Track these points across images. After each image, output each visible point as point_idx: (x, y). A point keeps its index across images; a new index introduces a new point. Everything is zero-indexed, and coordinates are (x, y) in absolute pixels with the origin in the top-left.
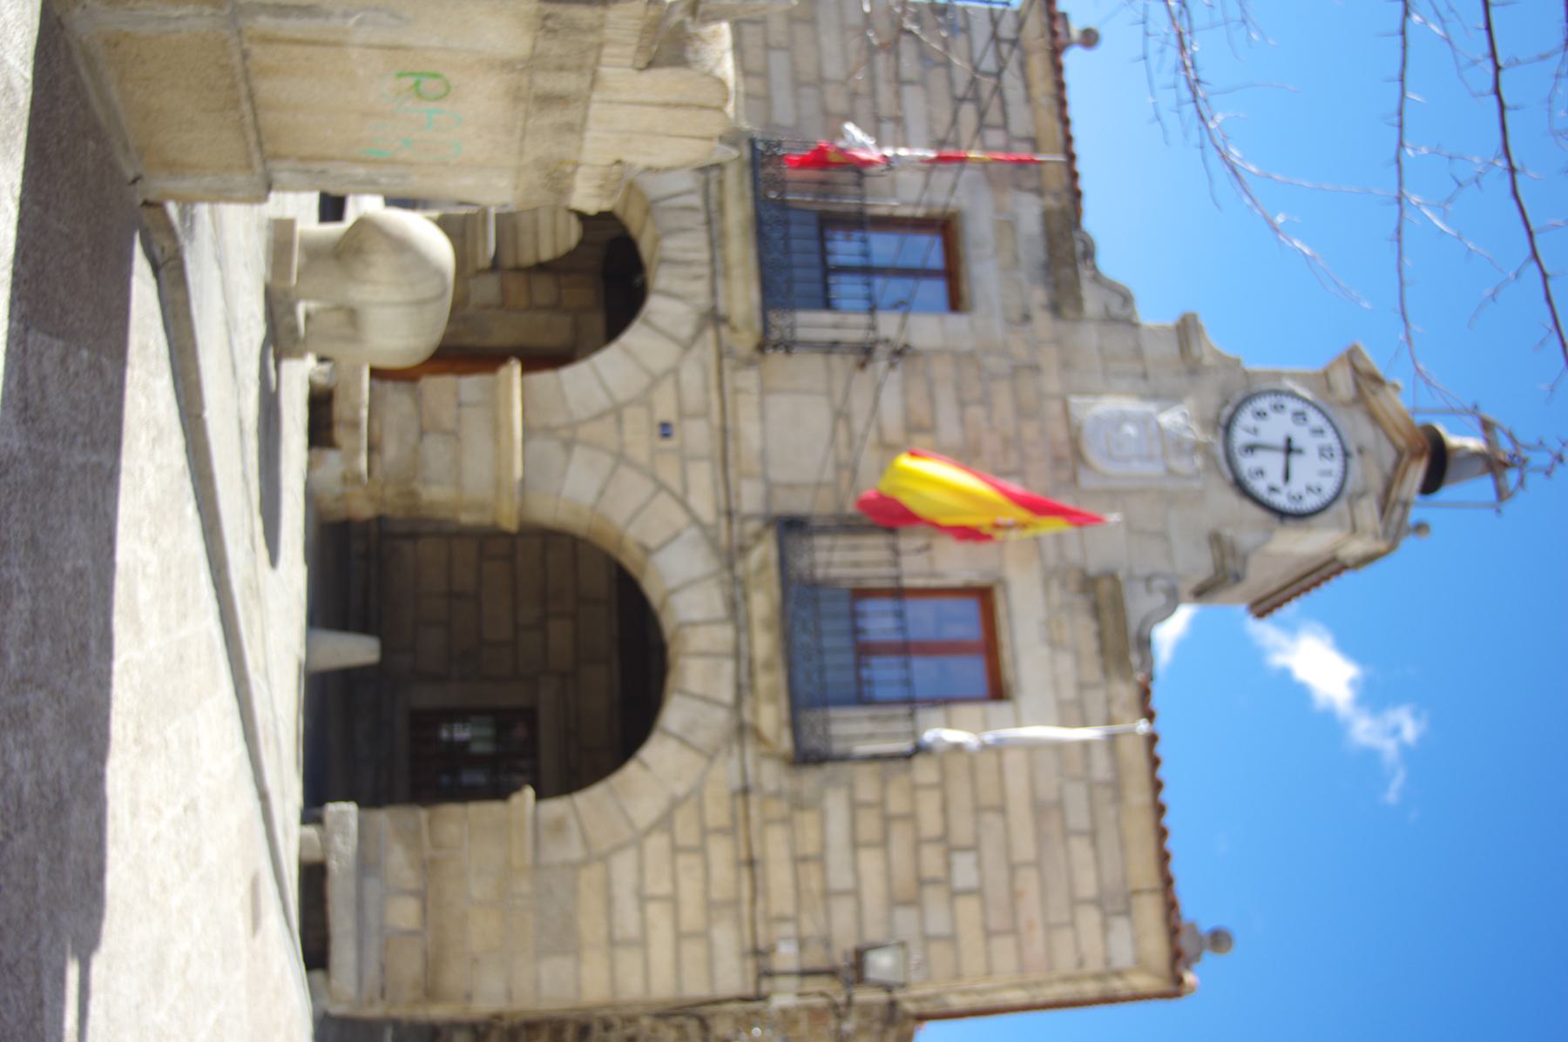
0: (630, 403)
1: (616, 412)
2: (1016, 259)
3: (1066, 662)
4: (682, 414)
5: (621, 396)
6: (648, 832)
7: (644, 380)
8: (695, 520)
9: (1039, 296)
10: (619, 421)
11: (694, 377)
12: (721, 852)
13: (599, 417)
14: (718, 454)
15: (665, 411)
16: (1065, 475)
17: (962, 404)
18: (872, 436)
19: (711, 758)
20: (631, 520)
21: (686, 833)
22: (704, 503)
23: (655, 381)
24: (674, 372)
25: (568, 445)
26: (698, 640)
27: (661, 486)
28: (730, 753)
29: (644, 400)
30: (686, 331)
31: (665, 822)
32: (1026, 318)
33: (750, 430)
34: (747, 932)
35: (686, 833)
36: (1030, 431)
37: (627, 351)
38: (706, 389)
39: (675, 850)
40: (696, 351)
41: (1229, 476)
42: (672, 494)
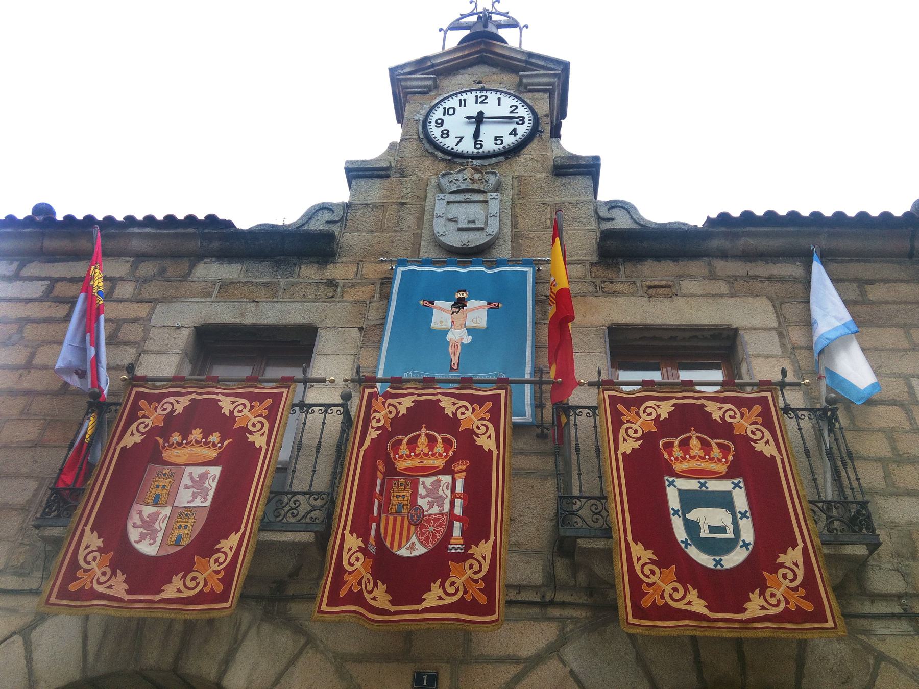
3: (688, 286)
8: (554, 650)
9: (309, 272)
19: (881, 658)
28: (869, 633)
30: (285, 641)
32: (331, 283)
41: (502, 158)
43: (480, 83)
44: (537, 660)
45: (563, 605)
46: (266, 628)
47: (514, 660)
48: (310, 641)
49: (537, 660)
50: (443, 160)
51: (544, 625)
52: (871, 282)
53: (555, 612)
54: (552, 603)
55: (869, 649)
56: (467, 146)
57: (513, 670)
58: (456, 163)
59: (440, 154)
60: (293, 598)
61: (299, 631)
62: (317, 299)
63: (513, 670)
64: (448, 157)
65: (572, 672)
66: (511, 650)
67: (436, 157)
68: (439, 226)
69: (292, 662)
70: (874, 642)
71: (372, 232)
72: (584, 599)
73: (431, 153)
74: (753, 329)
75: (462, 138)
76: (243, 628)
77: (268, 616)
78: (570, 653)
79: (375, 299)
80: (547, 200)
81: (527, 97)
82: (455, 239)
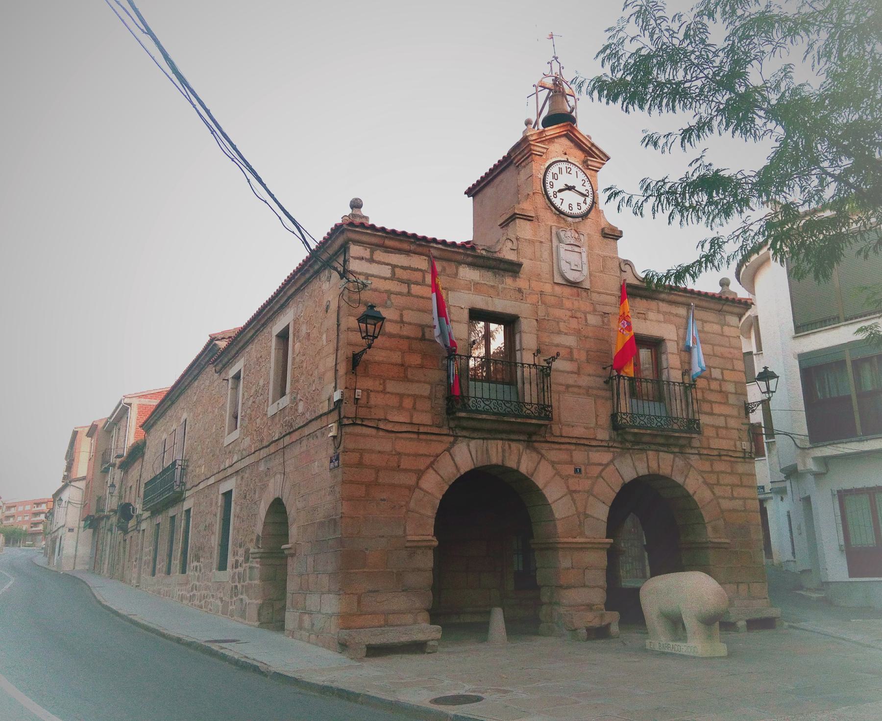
0: (568, 487)
1: (571, 492)
2: (492, 286)
4: (571, 463)
7: (557, 478)
8: (612, 461)
9: (509, 281)
10: (575, 491)
11: (554, 455)
12: (720, 466)
13: (574, 500)
14: (586, 448)
15: (569, 470)
16: (584, 294)
17: (559, 332)
19: (691, 466)
20: (614, 491)
21: (712, 479)
22: (606, 457)
23: (558, 473)
24: (553, 463)
25: (587, 516)
26: (654, 465)
27: (600, 475)
28: (689, 459)
29: (566, 478)
30: (534, 455)
31: (710, 486)
32: (520, 290)
33: (579, 431)
34: (739, 460)
35: (712, 479)
36: (567, 304)
37: (545, 486)
38: (560, 449)
39: (718, 484)
40: (543, 452)
41: (581, 219)
42: (603, 470)
43: (565, 154)
44: (607, 465)
45: (615, 447)
46: (528, 451)
47: (600, 464)
48: (542, 456)
49: (607, 465)
50: (555, 214)
51: (609, 454)
52: (706, 322)
53: (612, 449)
54: (612, 447)
55: (689, 463)
56: (551, 192)
57: (601, 468)
58: (560, 217)
59: (553, 209)
60: (536, 441)
61: (538, 452)
62: (516, 300)
63: (601, 468)
64: (558, 213)
65: (617, 469)
66: (600, 461)
67: (552, 210)
68: (565, 267)
69: (539, 463)
71: (531, 259)
73: (549, 207)
74: (670, 340)
75: (563, 200)
76: (521, 451)
77: (528, 447)
78: (616, 462)
79: (540, 303)
80: (601, 253)
81: (588, 172)
82: (572, 276)
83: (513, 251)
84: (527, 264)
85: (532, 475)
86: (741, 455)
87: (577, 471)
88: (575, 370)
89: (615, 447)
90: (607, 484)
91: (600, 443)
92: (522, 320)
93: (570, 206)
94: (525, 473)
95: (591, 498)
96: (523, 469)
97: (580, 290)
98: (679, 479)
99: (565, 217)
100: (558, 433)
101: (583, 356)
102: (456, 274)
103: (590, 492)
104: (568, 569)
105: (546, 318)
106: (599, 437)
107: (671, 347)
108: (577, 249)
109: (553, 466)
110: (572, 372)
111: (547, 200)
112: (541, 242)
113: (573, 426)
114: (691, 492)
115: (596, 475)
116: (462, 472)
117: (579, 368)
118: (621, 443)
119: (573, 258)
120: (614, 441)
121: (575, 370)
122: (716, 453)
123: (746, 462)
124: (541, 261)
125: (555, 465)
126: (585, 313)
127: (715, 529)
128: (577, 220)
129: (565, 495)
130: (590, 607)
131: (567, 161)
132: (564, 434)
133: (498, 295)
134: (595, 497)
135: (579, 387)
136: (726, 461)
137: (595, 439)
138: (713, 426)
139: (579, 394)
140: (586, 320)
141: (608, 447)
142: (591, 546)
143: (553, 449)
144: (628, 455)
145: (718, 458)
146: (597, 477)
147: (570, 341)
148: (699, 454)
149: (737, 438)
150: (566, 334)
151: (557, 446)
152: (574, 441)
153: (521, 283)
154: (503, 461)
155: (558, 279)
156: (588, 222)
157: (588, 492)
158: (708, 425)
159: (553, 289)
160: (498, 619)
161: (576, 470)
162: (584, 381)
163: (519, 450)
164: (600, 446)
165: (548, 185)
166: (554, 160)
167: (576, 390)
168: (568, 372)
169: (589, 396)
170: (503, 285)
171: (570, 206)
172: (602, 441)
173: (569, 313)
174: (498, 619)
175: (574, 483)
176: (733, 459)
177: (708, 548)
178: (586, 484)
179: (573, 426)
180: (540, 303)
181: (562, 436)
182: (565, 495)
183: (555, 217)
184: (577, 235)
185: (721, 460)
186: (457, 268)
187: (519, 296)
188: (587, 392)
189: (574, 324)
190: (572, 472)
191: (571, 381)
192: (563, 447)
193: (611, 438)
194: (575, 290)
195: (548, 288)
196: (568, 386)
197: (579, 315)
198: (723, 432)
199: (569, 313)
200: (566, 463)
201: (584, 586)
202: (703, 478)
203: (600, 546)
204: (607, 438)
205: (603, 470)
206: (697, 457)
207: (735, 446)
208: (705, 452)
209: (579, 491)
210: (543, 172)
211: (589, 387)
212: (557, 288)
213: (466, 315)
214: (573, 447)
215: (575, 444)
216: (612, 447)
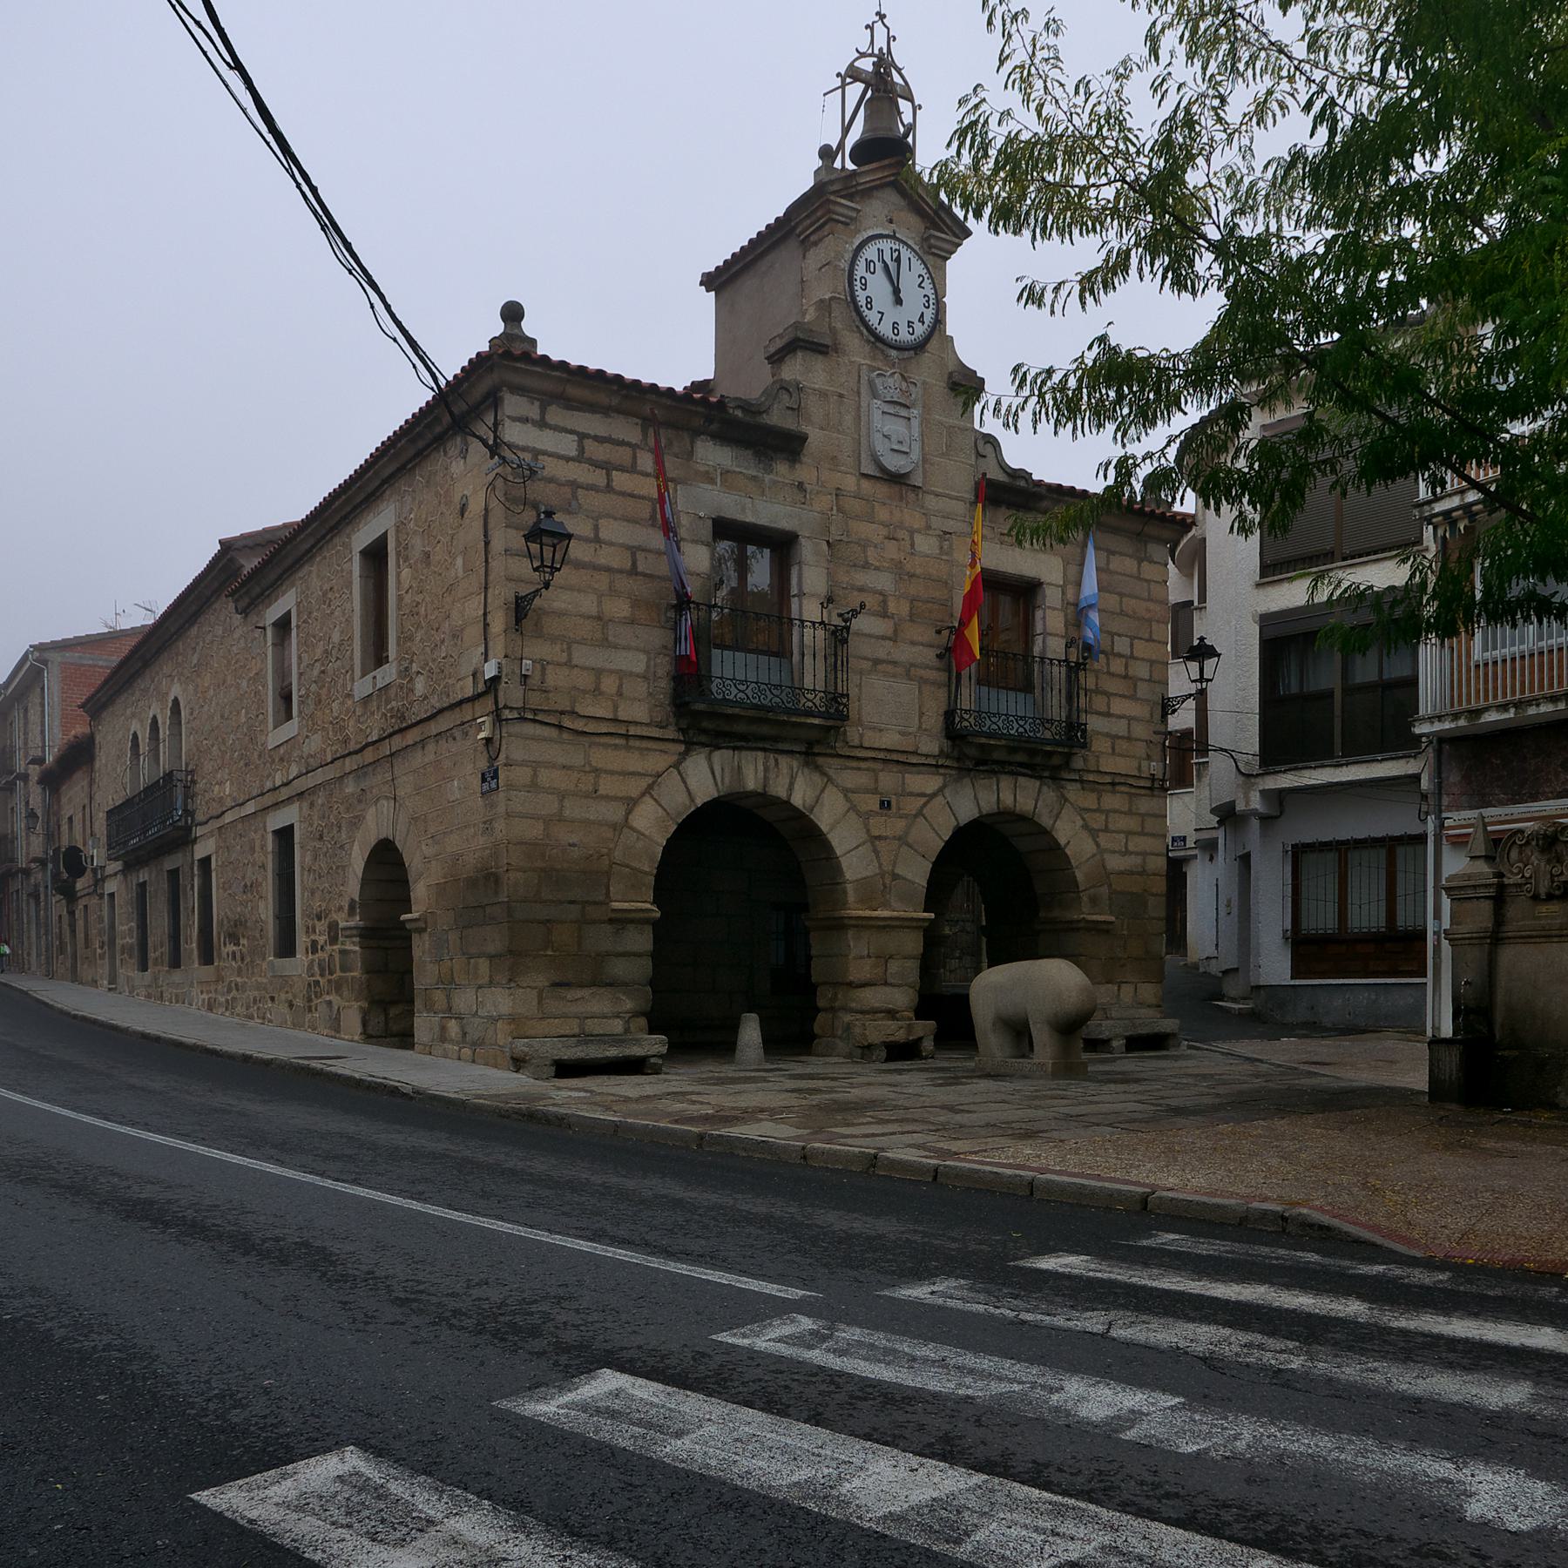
0: (868, 831)
2: (754, 478)
4: (875, 791)
5: (863, 836)
6: (1098, 845)
7: (852, 815)
8: (941, 790)
9: (781, 468)
10: (879, 838)
11: (851, 778)
12: (1112, 801)
13: (876, 852)
14: (900, 767)
15: (873, 803)
16: (911, 496)
17: (866, 566)
18: (888, 643)
19: (1066, 800)
21: (1097, 821)
22: (931, 783)
23: (853, 808)
24: (846, 792)
25: (895, 877)
26: (1007, 799)
27: (920, 813)
29: (865, 816)
30: (817, 777)
31: (1094, 834)
33: (890, 739)
34: (1143, 792)
35: (1097, 821)
36: (883, 514)
38: (859, 769)
39: (1106, 830)
40: (831, 772)
41: (912, 352)
42: (925, 805)
43: (891, 221)
44: (934, 795)
45: (947, 767)
46: (806, 770)
48: (830, 779)
49: (934, 795)
50: (868, 341)
52: (1113, 553)
53: (942, 771)
54: (942, 766)
59: (865, 331)
60: (819, 754)
61: (824, 774)
66: (923, 790)
67: (862, 334)
68: (881, 447)
69: (822, 791)
70: (1065, 792)
72: (955, 765)
77: (807, 764)
78: (947, 792)
81: (930, 260)
82: (894, 463)
83: (790, 412)
84: (815, 436)
85: (811, 810)
86: (1148, 784)
87: (885, 805)
88: (890, 633)
89: (947, 767)
90: (931, 825)
91: (923, 760)
92: (802, 541)
93: (895, 325)
94: (801, 808)
95: (904, 849)
96: (797, 800)
97: (904, 488)
98: (1046, 821)
99: (884, 348)
100: (856, 742)
101: (904, 609)
102: (691, 453)
103: (902, 840)
104: (862, 957)
105: (844, 538)
106: (924, 749)
107: (1052, 597)
108: (903, 412)
109: (845, 796)
110: (884, 638)
111: (854, 314)
112: (841, 396)
113: (881, 730)
114: (1062, 842)
115: (914, 812)
116: (699, 803)
117: (895, 631)
118: (958, 760)
119: (895, 427)
120: (947, 757)
121: (890, 633)
122: (1108, 779)
123: (1153, 796)
124: (839, 432)
125: (850, 795)
126: (912, 532)
127: (1094, 901)
128: (906, 354)
129: (864, 843)
130: (891, 1014)
131: (893, 237)
132: (866, 744)
133: (763, 494)
134: (910, 846)
135: (895, 663)
136: (1122, 792)
137: (915, 753)
138: (1108, 735)
139: (894, 676)
140: (912, 545)
141: (937, 766)
142: (898, 923)
143: (847, 768)
144: (967, 781)
145: (1109, 787)
146: (916, 816)
147: (884, 581)
148: (1082, 781)
149: (1144, 756)
150: (877, 569)
151: (854, 764)
152: (882, 755)
153: (805, 473)
154: (765, 786)
155: (869, 469)
156: (926, 358)
157: (899, 839)
158: (1098, 733)
159: (858, 485)
160: (750, 1033)
161: (882, 803)
162: (904, 653)
163: (791, 768)
164: (923, 764)
165: (858, 283)
166: (870, 233)
167: (890, 668)
168: (878, 637)
169: (911, 680)
170: (771, 476)
171: (895, 325)
172: (927, 756)
173: (884, 532)
174: (750, 1033)
175: (879, 825)
176: (1133, 791)
177: (1078, 929)
178: (898, 826)
179: (881, 730)
180: (834, 512)
181: (861, 747)
182: (864, 843)
183: (867, 348)
184: (904, 385)
185: (1114, 792)
186: (692, 443)
187: (800, 497)
188: (908, 671)
189: (891, 552)
190: (876, 807)
191: (881, 654)
192: (863, 765)
193: (941, 751)
194: (896, 488)
195: (850, 483)
196: (877, 662)
197: (902, 534)
198: (1123, 746)
199: (884, 532)
200: (867, 791)
201: (886, 984)
202: (1083, 819)
203: (915, 924)
204: (936, 751)
205: (925, 805)
206: (1078, 785)
207: (1139, 768)
208: (1091, 777)
209: (886, 838)
210: (848, 256)
211: (912, 665)
212: (865, 484)
213: (706, 530)
214: (878, 766)
215: (885, 761)
216: (942, 766)
